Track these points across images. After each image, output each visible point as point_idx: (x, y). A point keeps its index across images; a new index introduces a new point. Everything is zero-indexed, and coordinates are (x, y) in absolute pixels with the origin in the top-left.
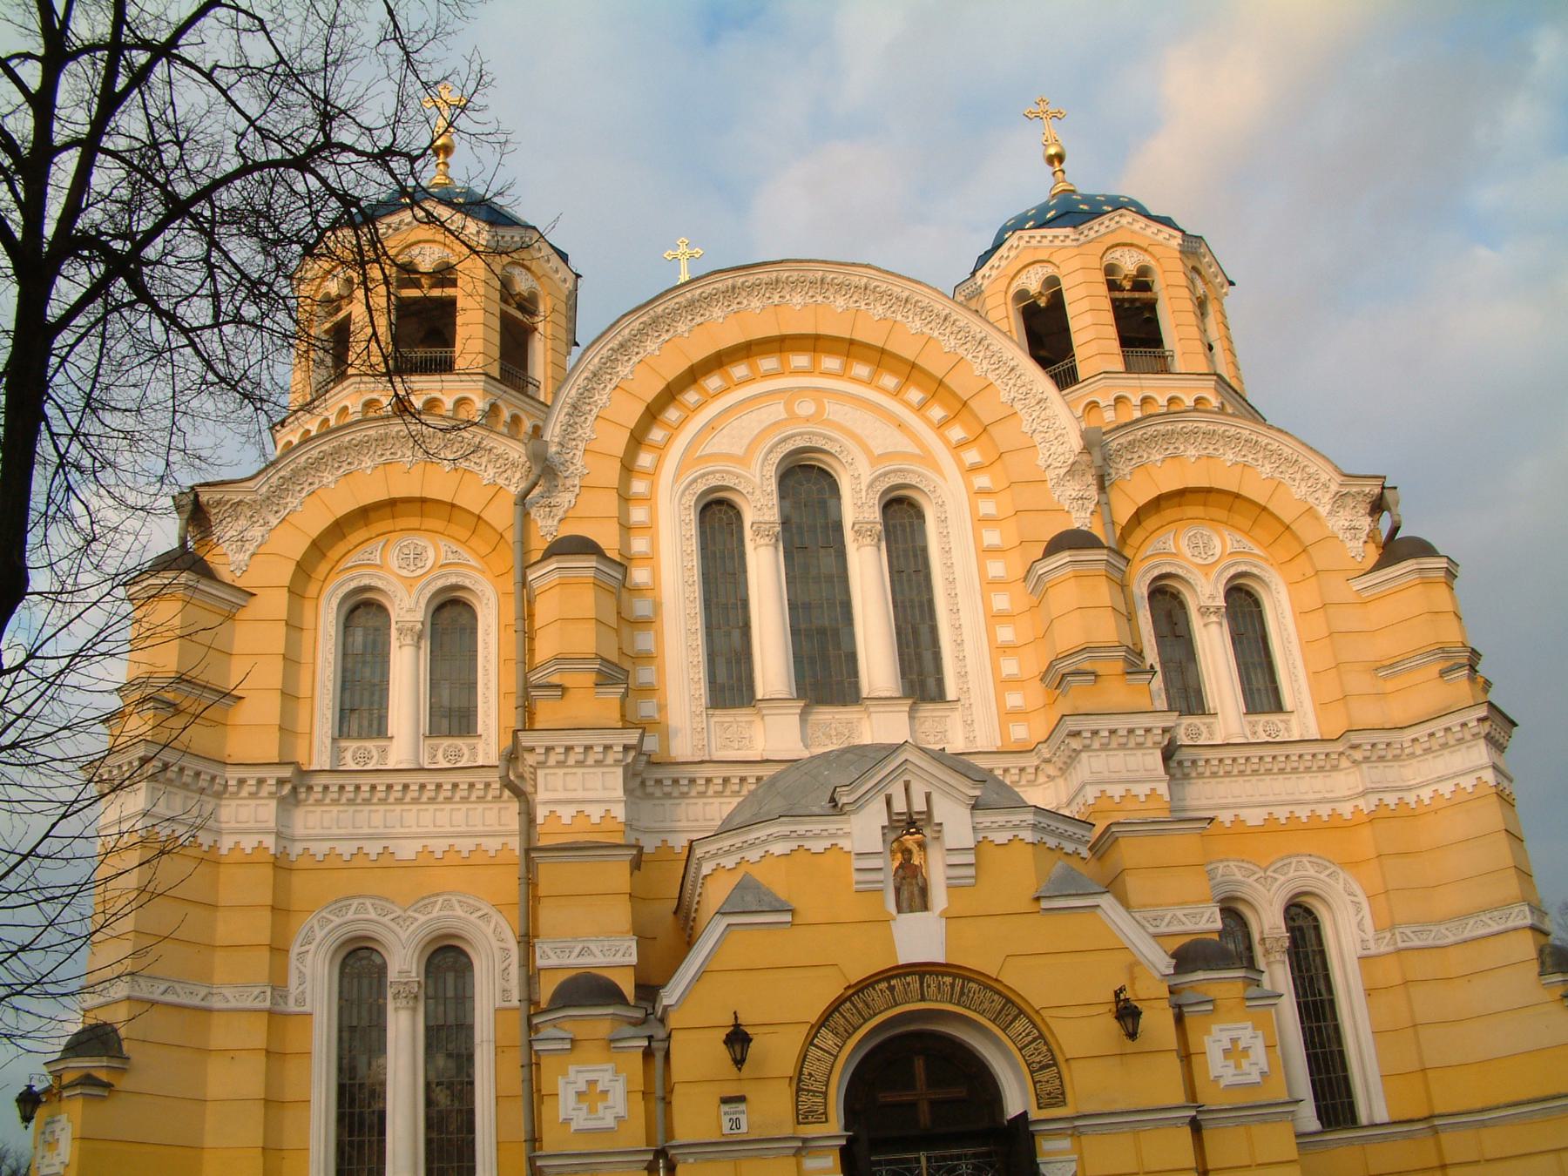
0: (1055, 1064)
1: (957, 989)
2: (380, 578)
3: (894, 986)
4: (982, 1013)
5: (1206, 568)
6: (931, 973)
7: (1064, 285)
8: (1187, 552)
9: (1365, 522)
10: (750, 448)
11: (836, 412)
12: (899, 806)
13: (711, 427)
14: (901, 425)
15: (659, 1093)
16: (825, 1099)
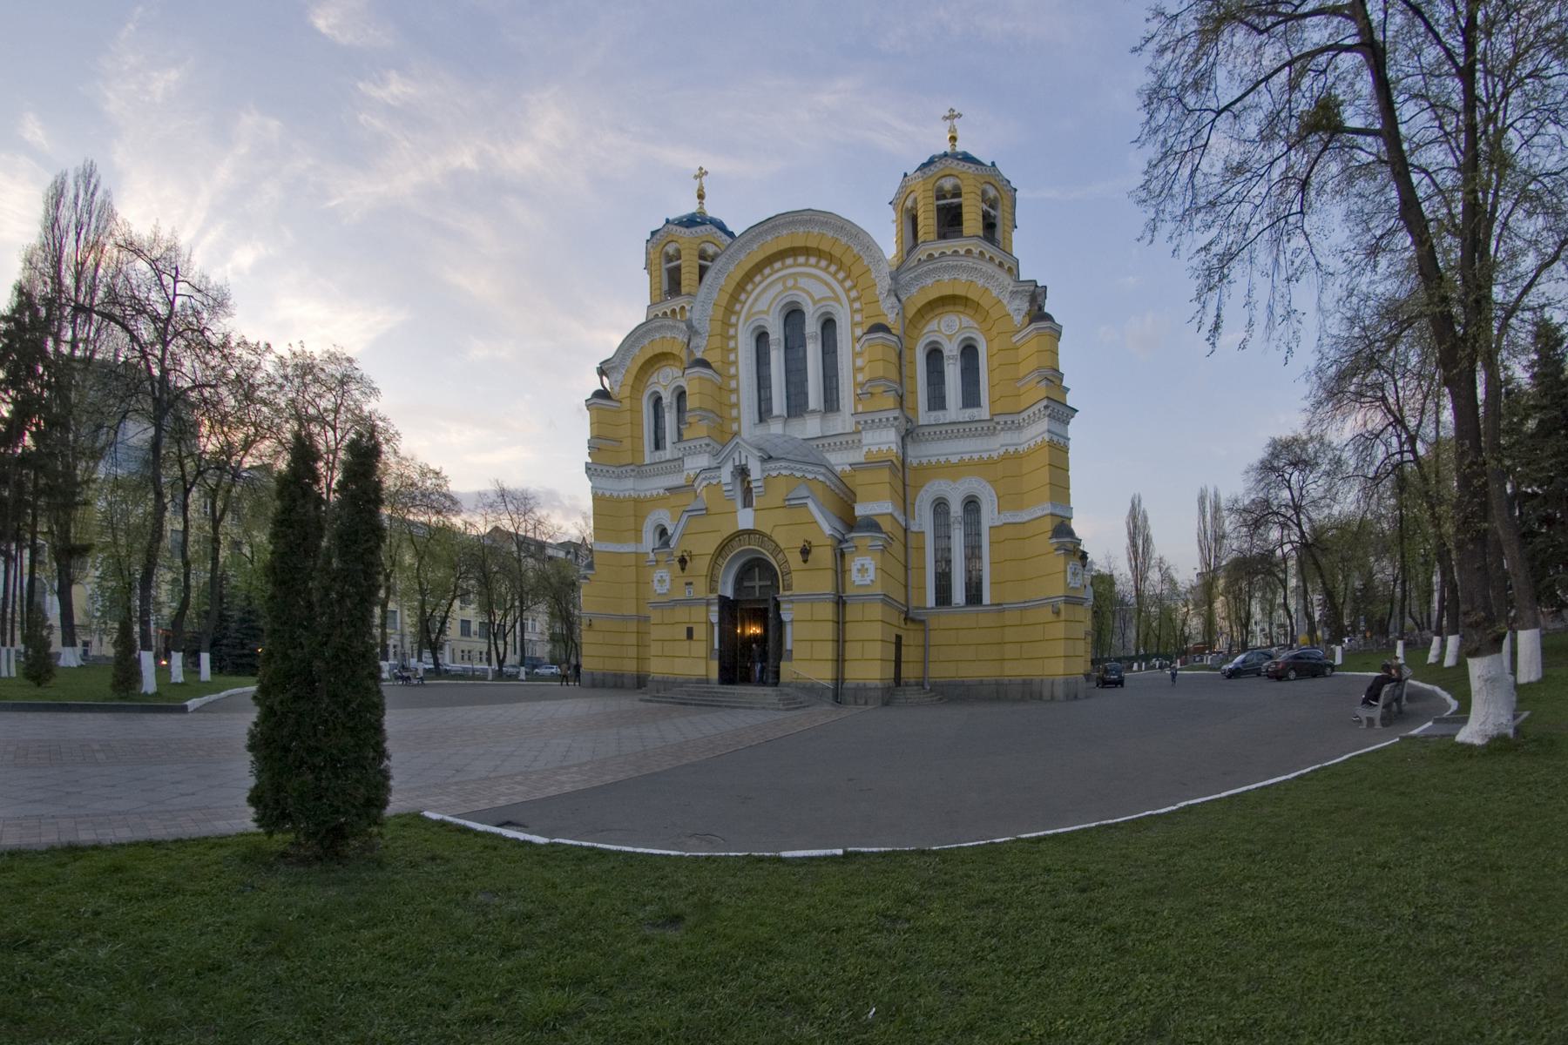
5: (950, 337)
8: (943, 330)
9: (1025, 306)
10: (769, 307)
11: (803, 282)
13: (756, 300)
14: (827, 284)
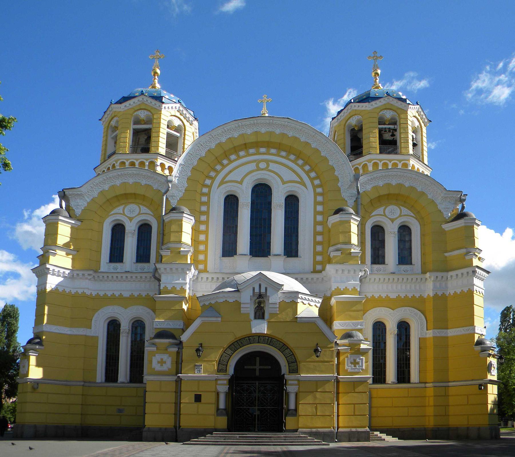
0: (296, 362)
7: (363, 123)
11: (272, 166)
13: (230, 172)
14: (294, 171)
15: (180, 362)
16: (227, 366)
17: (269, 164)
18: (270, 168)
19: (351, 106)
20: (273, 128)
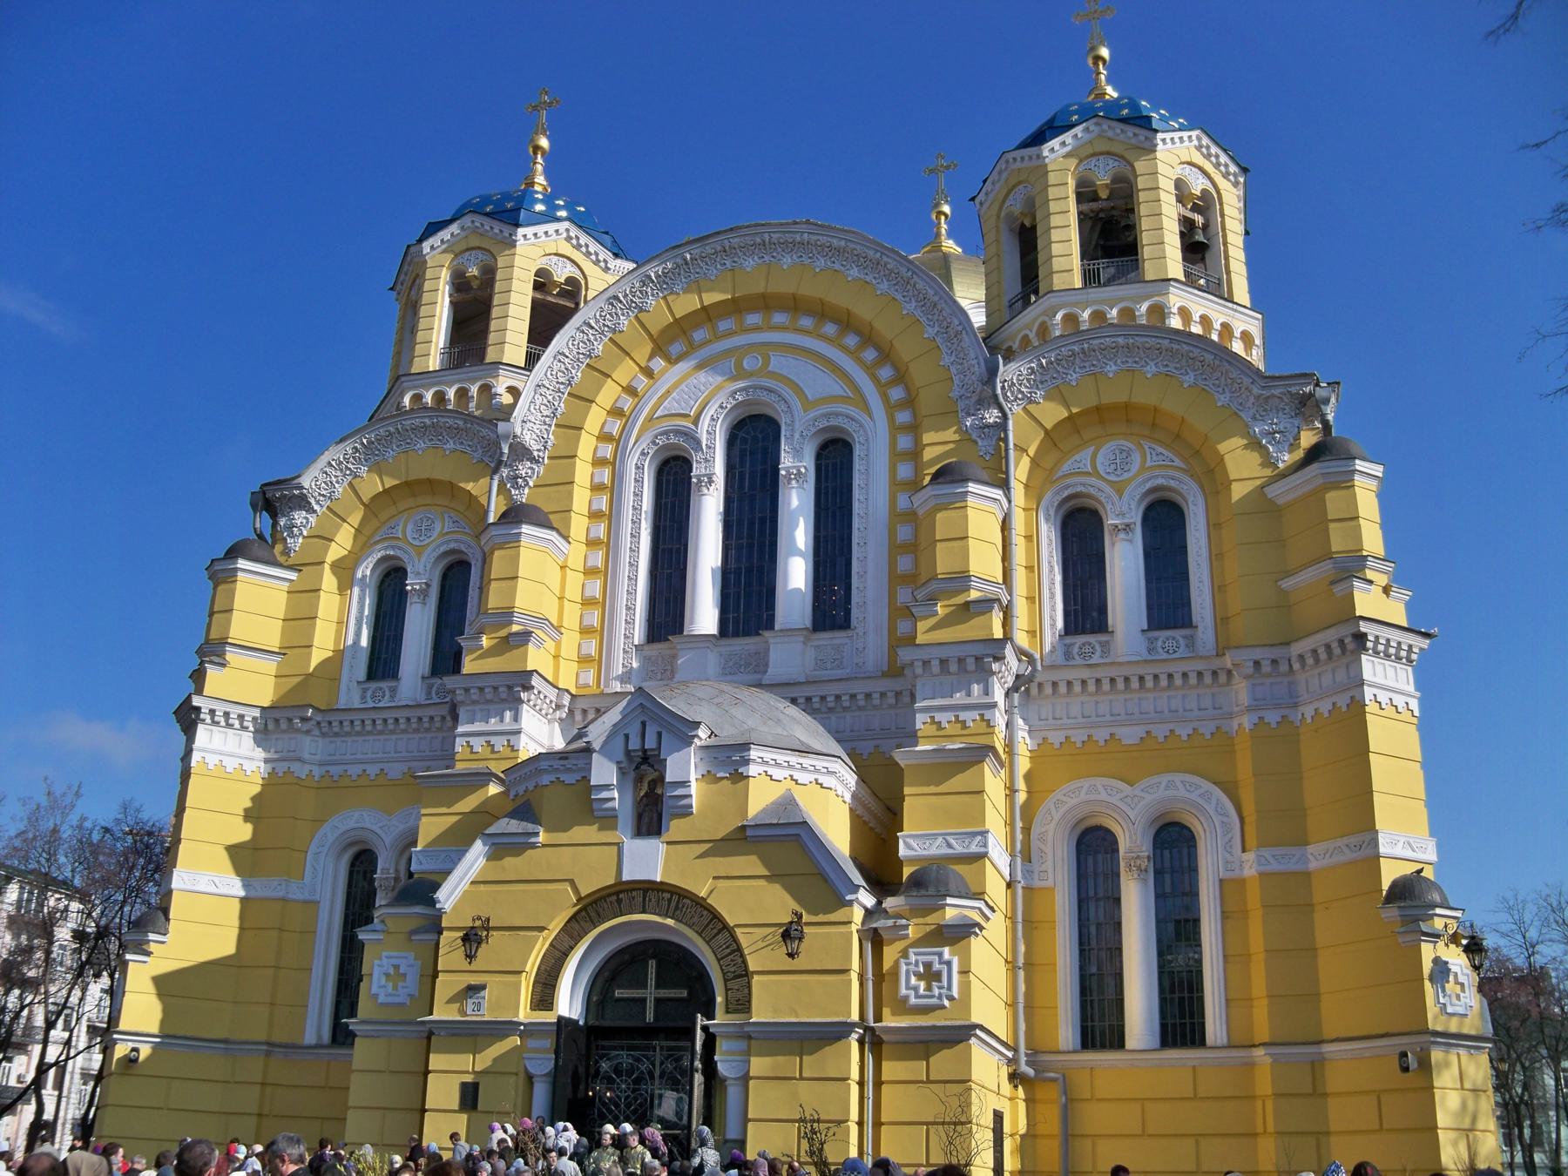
0: (747, 975)
1: (673, 904)
2: (400, 548)
3: (622, 900)
4: (690, 926)
6: (653, 890)
11: (777, 362)
12: (634, 744)
17: (770, 358)
18: (770, 369)
19: (1007, 162)
20: (775, 254)
